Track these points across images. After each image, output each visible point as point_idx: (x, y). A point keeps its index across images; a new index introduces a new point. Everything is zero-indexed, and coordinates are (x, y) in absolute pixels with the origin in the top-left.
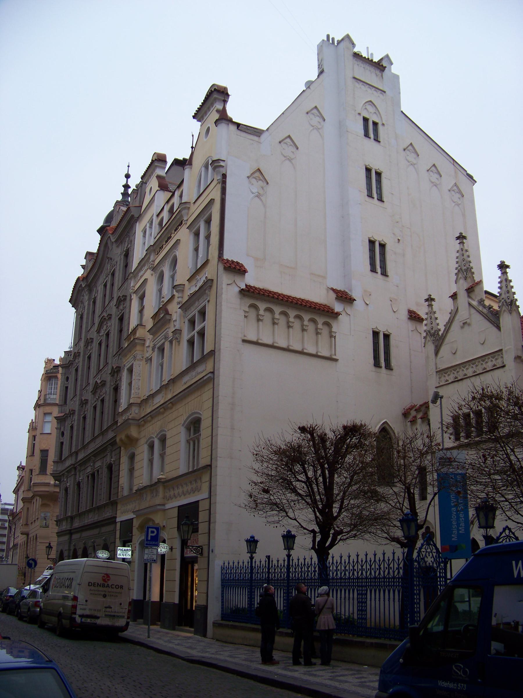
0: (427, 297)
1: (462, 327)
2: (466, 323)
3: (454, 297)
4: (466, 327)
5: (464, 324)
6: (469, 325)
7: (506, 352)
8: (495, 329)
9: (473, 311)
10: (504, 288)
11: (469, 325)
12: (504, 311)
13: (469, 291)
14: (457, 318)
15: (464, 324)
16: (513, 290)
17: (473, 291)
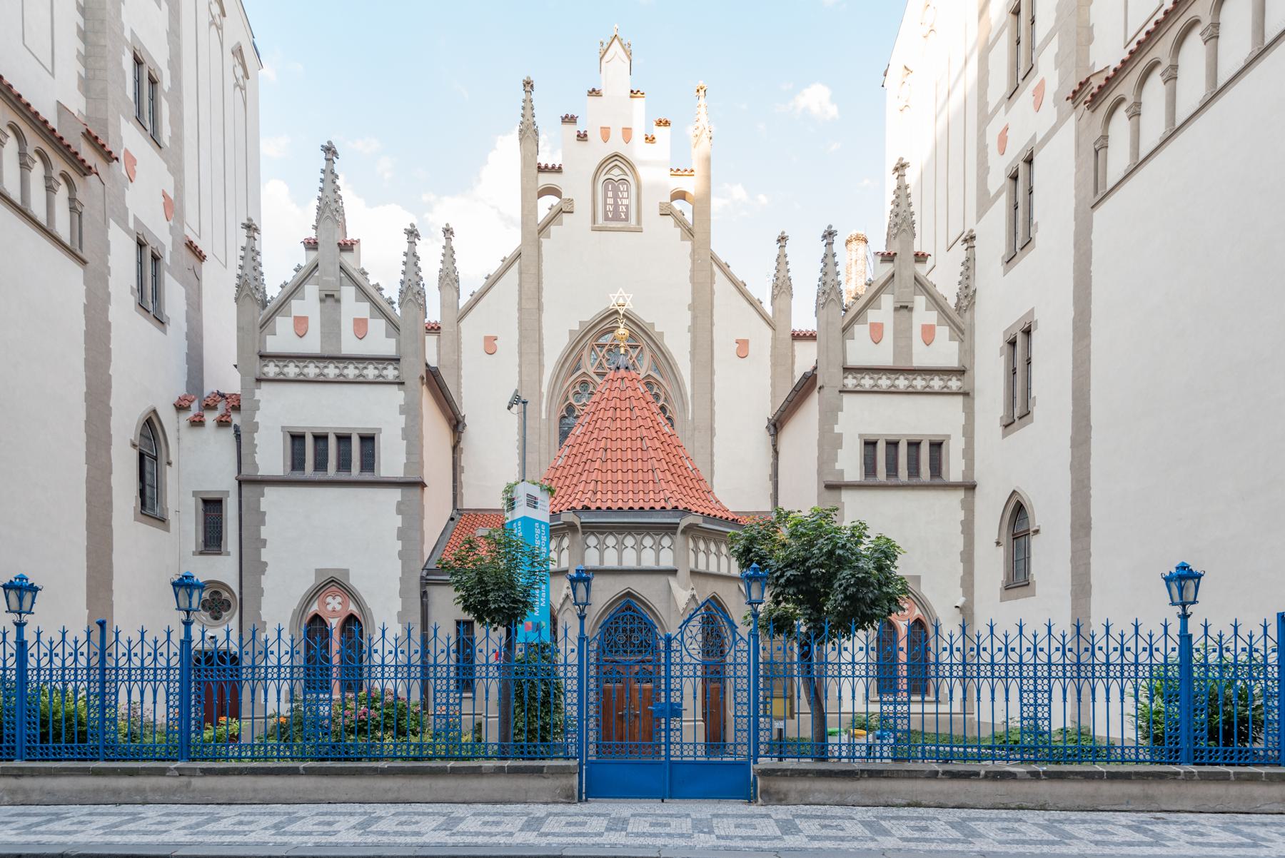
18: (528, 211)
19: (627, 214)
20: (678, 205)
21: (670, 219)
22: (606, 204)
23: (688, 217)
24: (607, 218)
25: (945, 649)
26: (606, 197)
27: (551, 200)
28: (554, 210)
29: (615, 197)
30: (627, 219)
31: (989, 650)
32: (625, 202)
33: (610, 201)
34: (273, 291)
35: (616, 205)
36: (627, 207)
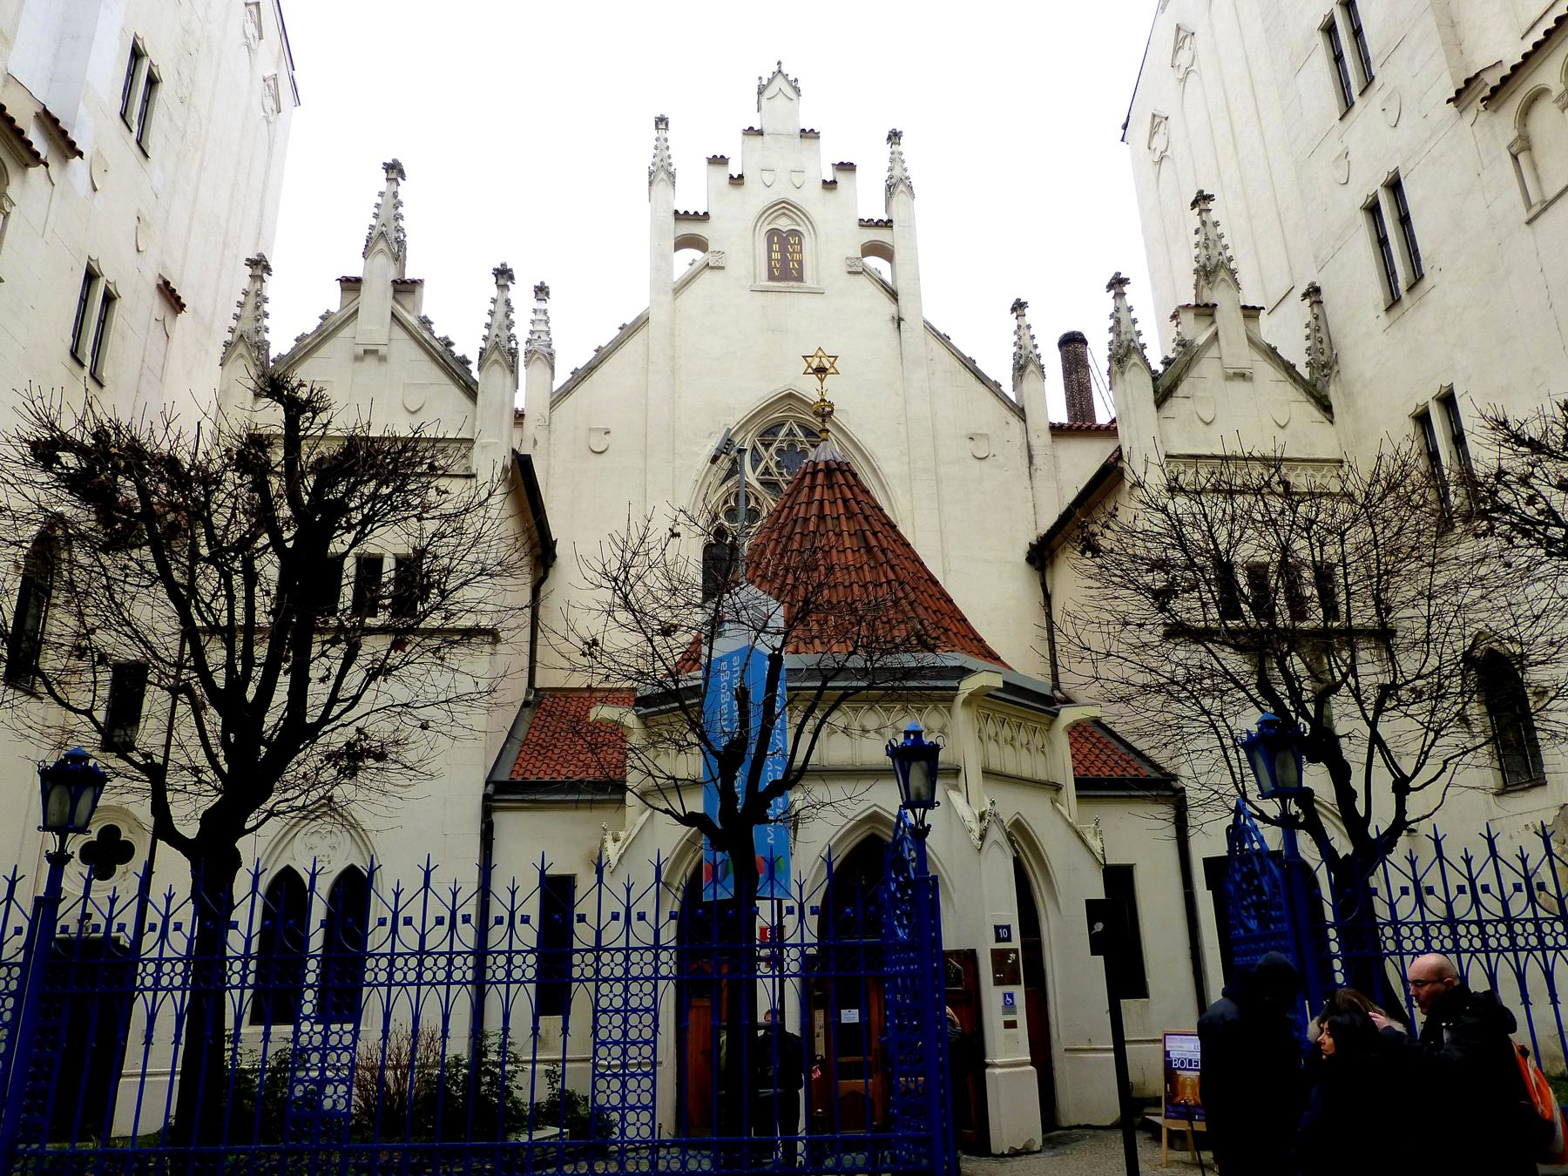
0: (253, 256)
1: (358, 358)
2: (375, 352)
3: (350, 285)
4: (370, 361)
5: (366, 352)
6: (383, 359)
7: (484, 447)
8: (455, 394)
9: (399, 333)
10: (500, 315)
11: (383, 359)
12: (496, 361)
13: (401, 287)
14: (346, 332)
15: (366, 352)
16: (486, 332)
17: (413, 292)
18: (660, 267)
19: (800, 270)
20: (874, 262)
21: (862, 280)
22: (770, 259)
23: (887, 277)
24: (771, 277)
25: (1461, 889)
26: (770, 250)
27: (691, 254)
28: (696, 265)
29: (783, 251)
30: (800, 279)
31: (1494, 888)
32: (796, 256)
33: (776, 256)
34: (280, 343)
35: (784, 261)
36: (800, 263)
